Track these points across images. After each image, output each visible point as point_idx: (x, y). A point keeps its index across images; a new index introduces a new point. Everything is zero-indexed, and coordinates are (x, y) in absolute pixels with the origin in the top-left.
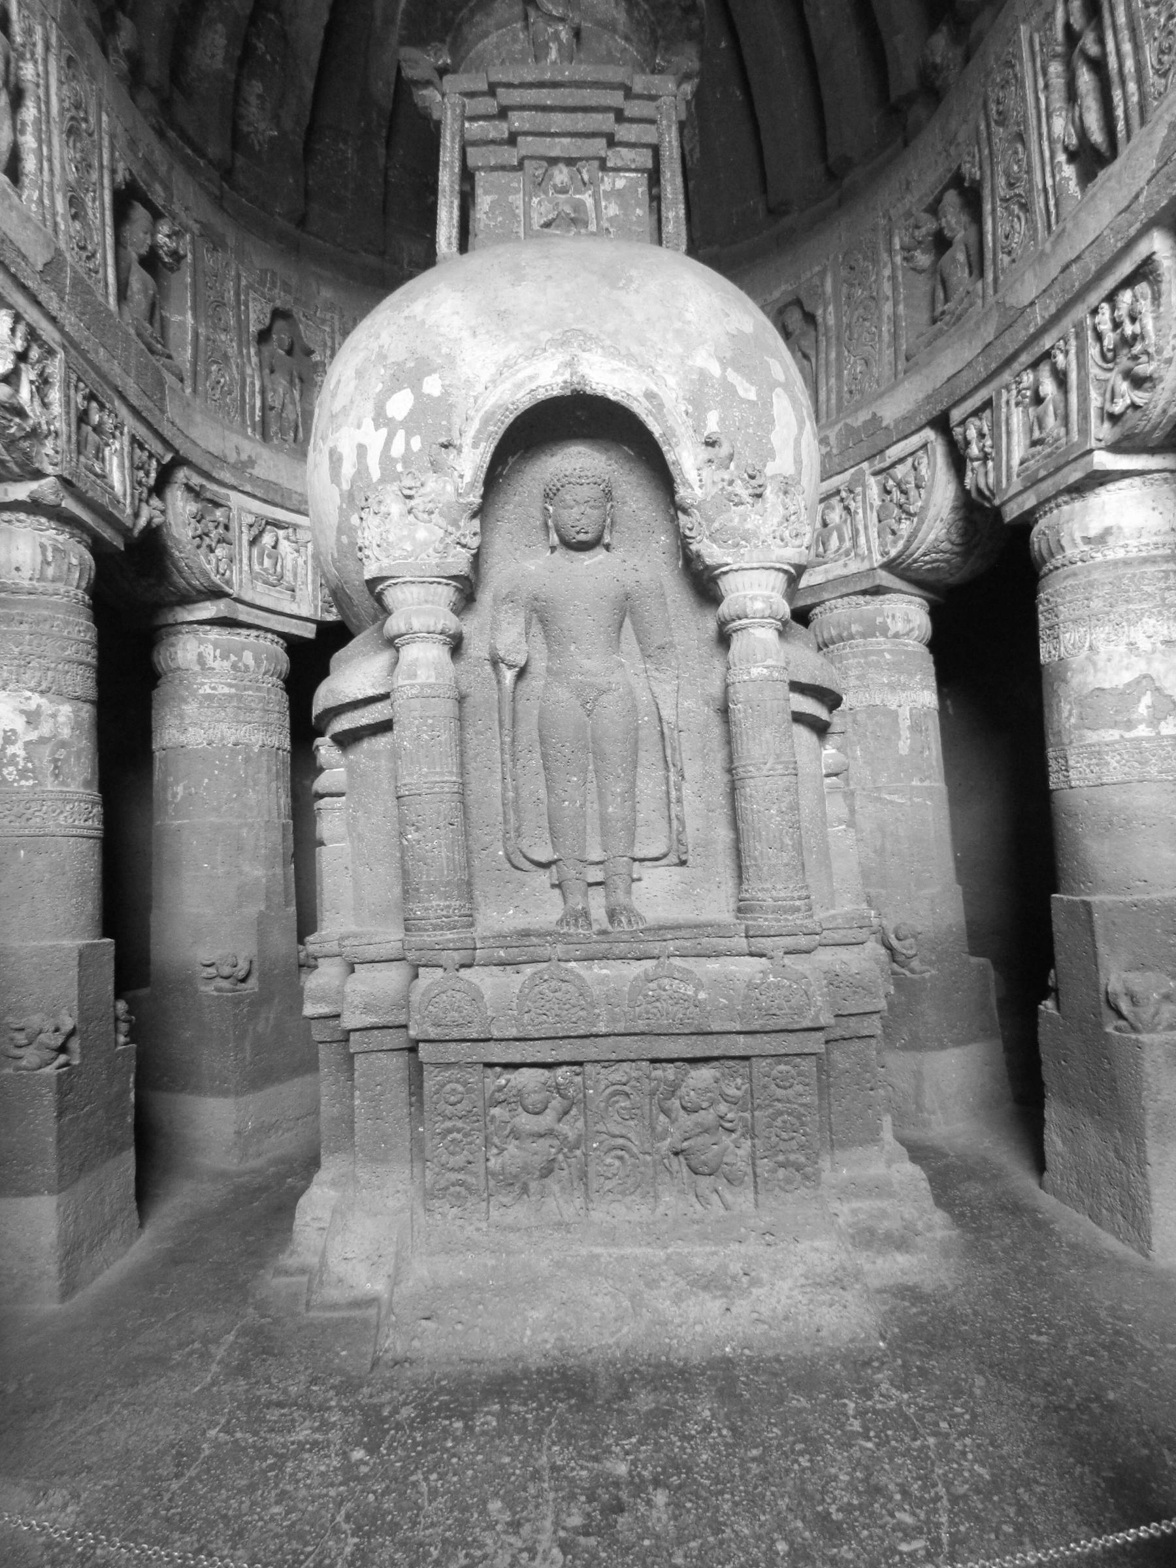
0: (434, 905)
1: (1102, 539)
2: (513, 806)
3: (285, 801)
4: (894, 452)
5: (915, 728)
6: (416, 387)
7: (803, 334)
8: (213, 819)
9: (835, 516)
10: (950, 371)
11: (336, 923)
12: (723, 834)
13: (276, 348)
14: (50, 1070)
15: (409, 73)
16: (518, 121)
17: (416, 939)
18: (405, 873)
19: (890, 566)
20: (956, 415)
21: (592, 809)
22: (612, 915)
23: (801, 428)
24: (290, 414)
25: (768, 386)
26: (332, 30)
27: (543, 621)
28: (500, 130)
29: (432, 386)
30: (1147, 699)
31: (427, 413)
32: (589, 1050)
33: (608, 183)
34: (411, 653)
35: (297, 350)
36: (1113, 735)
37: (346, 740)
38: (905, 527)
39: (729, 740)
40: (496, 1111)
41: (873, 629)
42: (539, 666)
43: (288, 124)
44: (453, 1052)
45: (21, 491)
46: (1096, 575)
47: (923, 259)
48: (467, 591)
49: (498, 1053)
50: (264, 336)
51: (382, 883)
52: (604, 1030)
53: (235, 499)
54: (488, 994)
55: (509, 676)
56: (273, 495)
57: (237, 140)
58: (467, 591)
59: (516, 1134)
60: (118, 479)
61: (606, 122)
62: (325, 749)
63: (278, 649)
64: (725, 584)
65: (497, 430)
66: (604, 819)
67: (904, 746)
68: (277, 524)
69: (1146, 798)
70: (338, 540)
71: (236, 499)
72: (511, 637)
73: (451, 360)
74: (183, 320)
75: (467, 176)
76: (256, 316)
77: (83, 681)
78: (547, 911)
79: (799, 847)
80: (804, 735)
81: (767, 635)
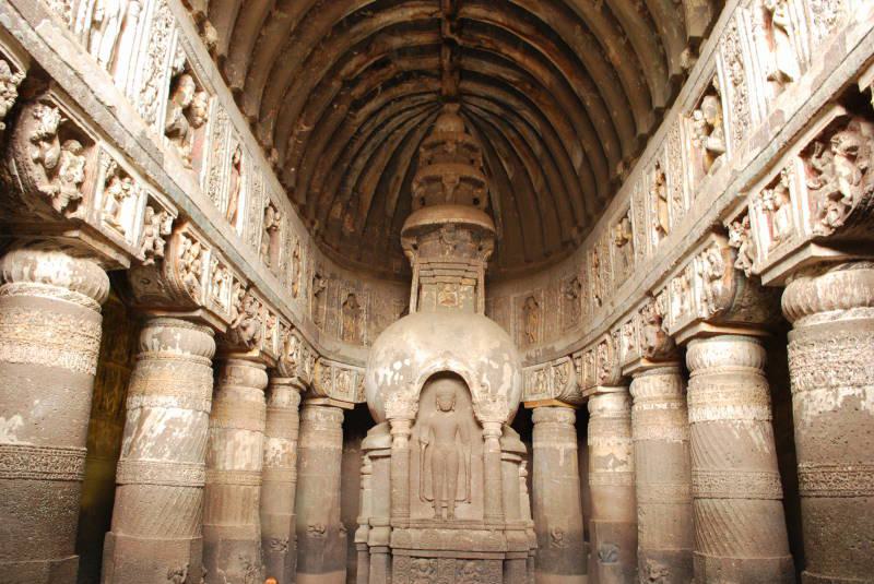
0: (399, 510)
1: (602, 411)
2: (422, 484)
3: (339, 468)
4: (559, 361)
5: (566, 456)
6: (402, 361)
7: (534, 310)
8: (316, 475)
9: (541, 378)
10: (572, 342)
11: (364, 517)
12: (481, 495)
13: (348, 307)
14: (283, 552)
15: (405, 247)
16: (435, 272)
17: (393, 520)
18: (391, 501)
19: (556, 399)
20: (575, 355)
21: (445, 485)
22: (449, 516)
23: (513, 371)
24: (352, 329)
25: (502, 363)
26: (374, 196)
27: (435, 433)
28: (431, 273)
29: (407, 362)
30: (612, 460)
31: (405, 370)
32: (440, 554)
33: (462, 289)
34: (396, 440)
35: (356, 306)
36: (602, 470)
37: (372, 458)
38: (562, 387)
39: (484, 468)
40: (413, 571)
41: (553, 420)
42: (432, 443)
43: (358, 227)
44: (401, 552)
45: (287, 381)
46: (601, 422)
47: (570, 297)
48: (413, 422)
49: (414, 553)
50: (345, 304)
51: (383, 503)
52: (443, 548)
53: (333, 364)
54: (413, 536)
55: (424, 446)
56: (345, 360)
57: (341, 236)
58: (413, 422)
59: (417, 577)
60: (307, 370)
61: (463, 273)
62: (366, 460)
63: (340, 413)
64: (484, 425)
65: (425, 379)
66: (448, 488)
67: (561, 462)
68: (345, 370)
69: (611, 491)
70: (377, 395)
71: (333, 364)
72: (425, 436)
73: (413, 356)
74: (324, 308)
75: (420, 288)
76: (344, 297)
77: (295, 435)
78: (430, 514)
79: (502, 500)
80: (511, 465)
81: (495, 440)
